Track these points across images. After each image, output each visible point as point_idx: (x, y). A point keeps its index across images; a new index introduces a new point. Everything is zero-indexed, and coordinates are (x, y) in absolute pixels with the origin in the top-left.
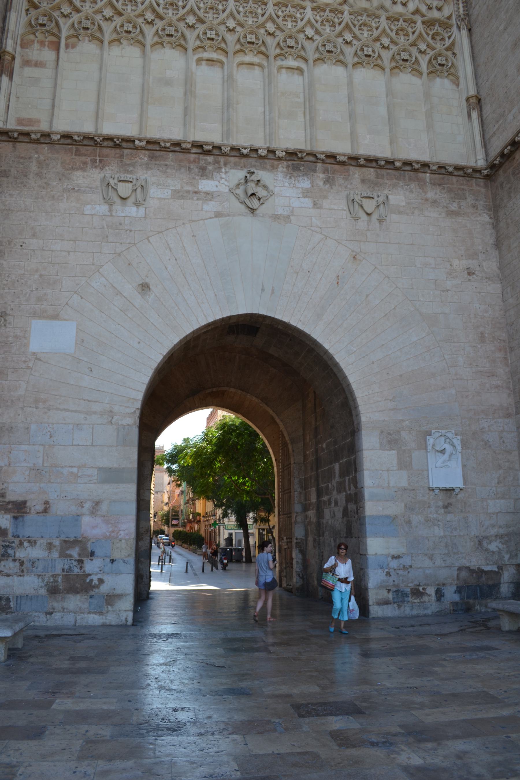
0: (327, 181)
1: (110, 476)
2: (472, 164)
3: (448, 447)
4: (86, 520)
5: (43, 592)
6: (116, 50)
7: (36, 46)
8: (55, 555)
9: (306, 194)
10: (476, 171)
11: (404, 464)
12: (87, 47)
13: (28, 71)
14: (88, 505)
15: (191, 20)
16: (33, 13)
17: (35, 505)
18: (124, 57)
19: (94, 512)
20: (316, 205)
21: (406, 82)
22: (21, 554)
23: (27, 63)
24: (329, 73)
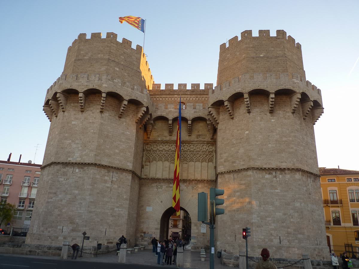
0: (189, 184)
1: (156, 229)
2: (213, 179)
3: (204, 227)
4: (153, 235)
5: (147, 244)
6: (158, 162)
7: (147, 162)
8: (149, 239)
9: (186, 186)
10: (213, 180)
11: (197, 229)
12: (154, 162)
13: (146, 167)
14: (153, 233)
15: (170, 156)
16: (147, 156)
17: (147, 232)
18: (160, 163)
19: (154, 234)
20: (187, 188)
21: (205, 164)
22: (145, 239)
23: (146, 165)
24: (192, 163)
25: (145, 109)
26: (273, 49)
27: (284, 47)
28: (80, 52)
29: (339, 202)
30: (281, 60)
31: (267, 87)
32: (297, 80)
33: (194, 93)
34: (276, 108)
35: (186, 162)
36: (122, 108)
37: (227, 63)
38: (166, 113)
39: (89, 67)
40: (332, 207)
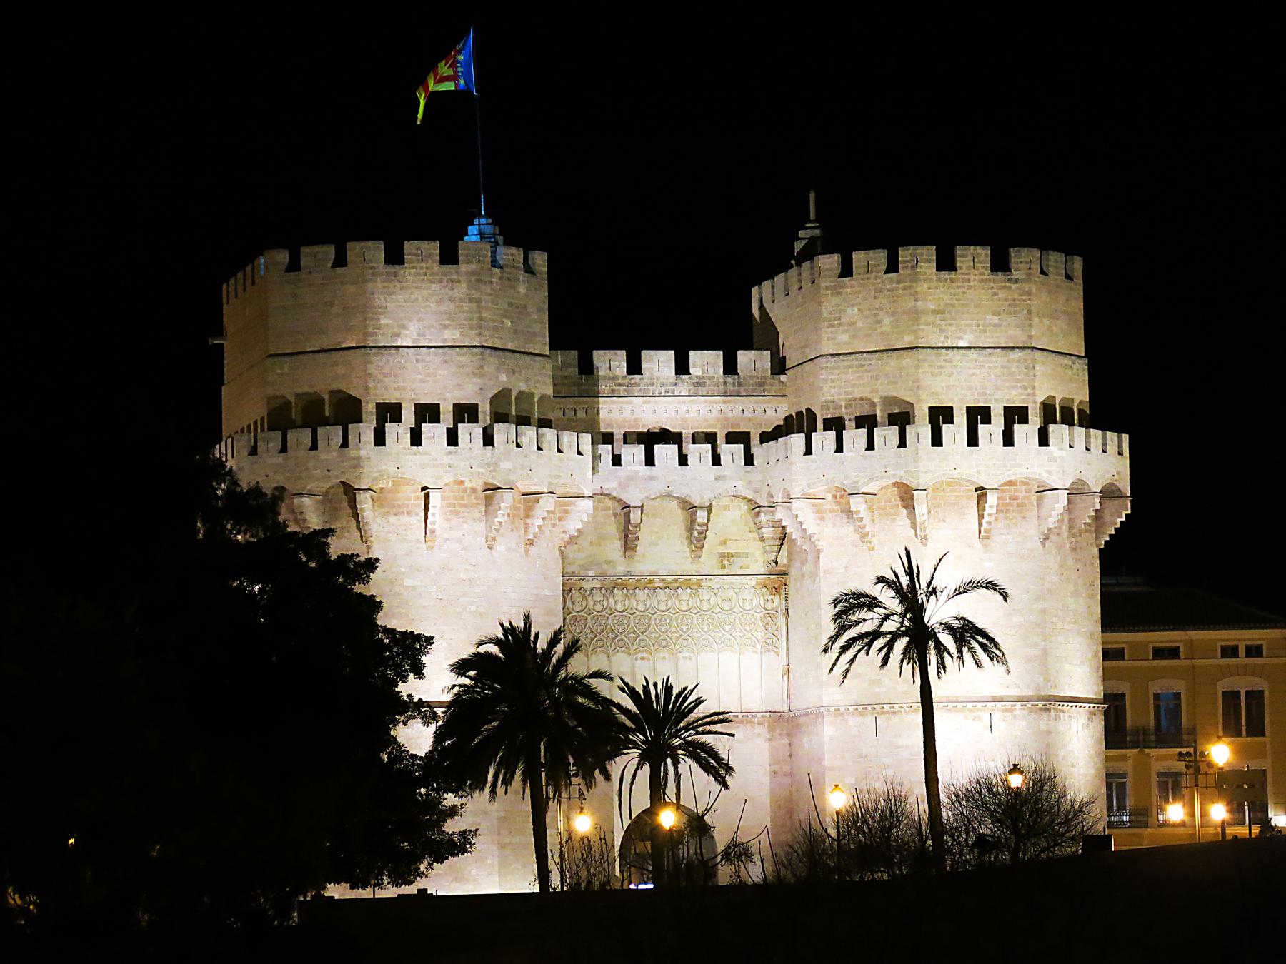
25: (587, 505)
26: (996, 319)
27: (1029, 312)
28: (379, 320)
29: (1185, 737)
30: (1018, 361)
31: (978, 472)
32: (1061, 449)
33: (703, 390)
34: (1000, 525)
35: (687, 654)
36: (540, 522)
37: (844, 337)
38: (620, 484)
39: (423, 381)
40: (1159, 758)
